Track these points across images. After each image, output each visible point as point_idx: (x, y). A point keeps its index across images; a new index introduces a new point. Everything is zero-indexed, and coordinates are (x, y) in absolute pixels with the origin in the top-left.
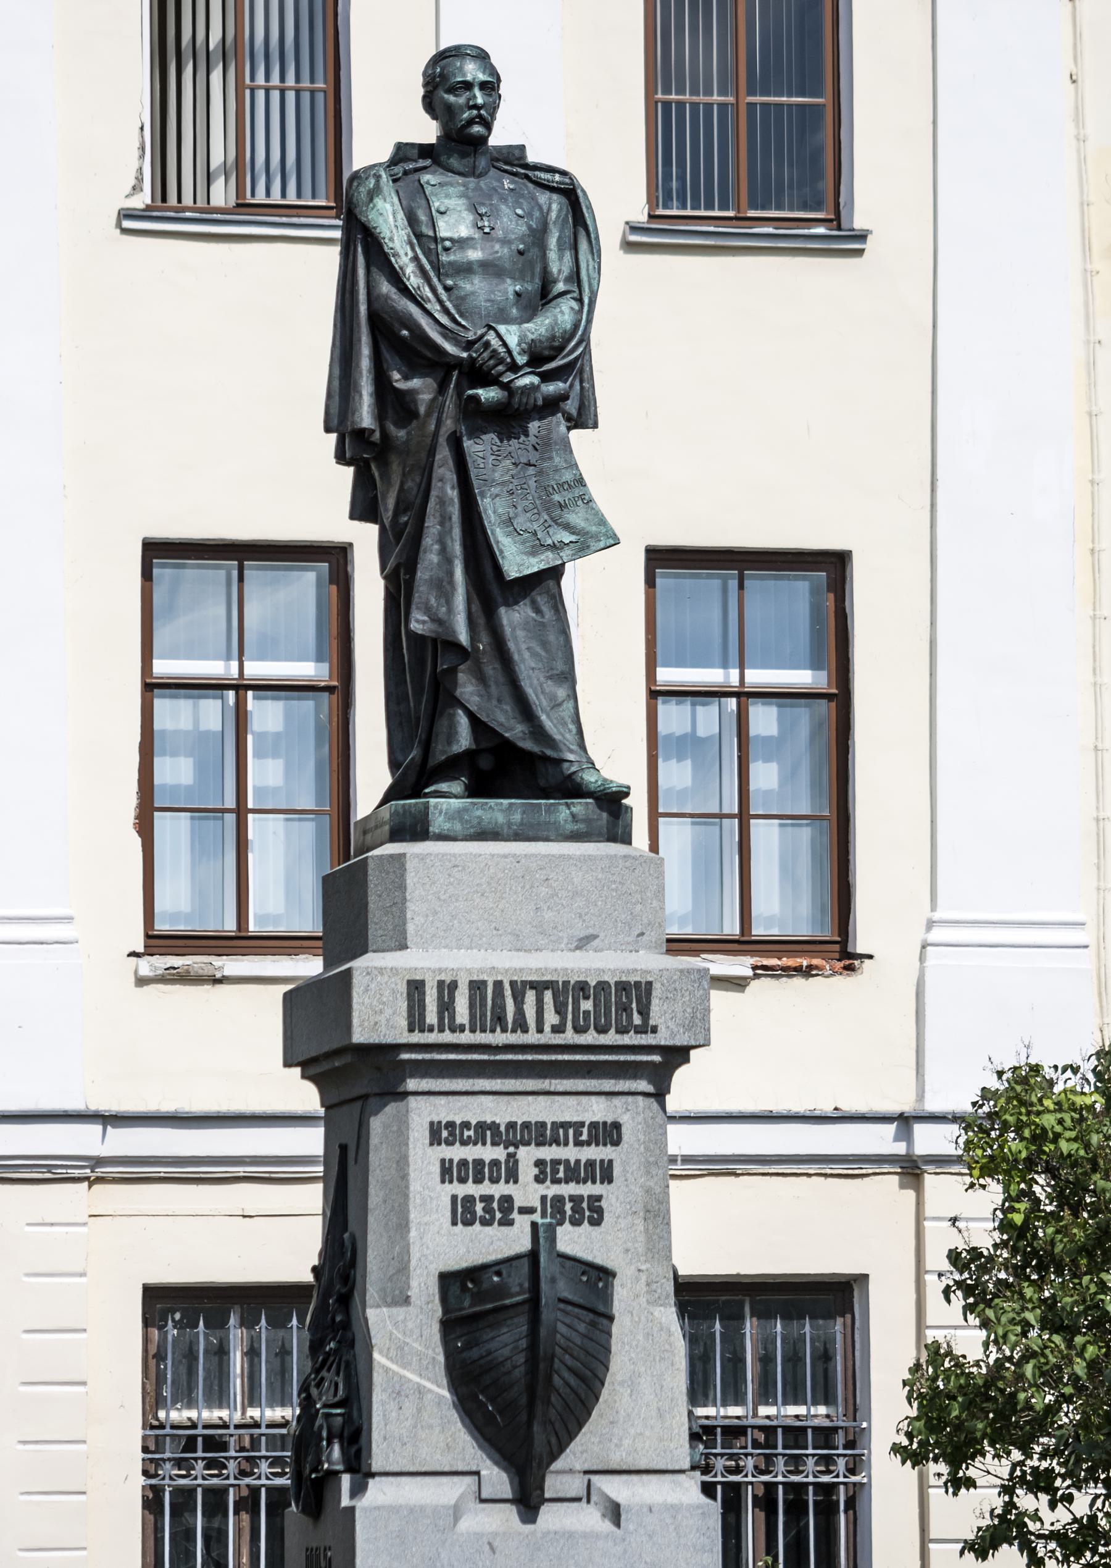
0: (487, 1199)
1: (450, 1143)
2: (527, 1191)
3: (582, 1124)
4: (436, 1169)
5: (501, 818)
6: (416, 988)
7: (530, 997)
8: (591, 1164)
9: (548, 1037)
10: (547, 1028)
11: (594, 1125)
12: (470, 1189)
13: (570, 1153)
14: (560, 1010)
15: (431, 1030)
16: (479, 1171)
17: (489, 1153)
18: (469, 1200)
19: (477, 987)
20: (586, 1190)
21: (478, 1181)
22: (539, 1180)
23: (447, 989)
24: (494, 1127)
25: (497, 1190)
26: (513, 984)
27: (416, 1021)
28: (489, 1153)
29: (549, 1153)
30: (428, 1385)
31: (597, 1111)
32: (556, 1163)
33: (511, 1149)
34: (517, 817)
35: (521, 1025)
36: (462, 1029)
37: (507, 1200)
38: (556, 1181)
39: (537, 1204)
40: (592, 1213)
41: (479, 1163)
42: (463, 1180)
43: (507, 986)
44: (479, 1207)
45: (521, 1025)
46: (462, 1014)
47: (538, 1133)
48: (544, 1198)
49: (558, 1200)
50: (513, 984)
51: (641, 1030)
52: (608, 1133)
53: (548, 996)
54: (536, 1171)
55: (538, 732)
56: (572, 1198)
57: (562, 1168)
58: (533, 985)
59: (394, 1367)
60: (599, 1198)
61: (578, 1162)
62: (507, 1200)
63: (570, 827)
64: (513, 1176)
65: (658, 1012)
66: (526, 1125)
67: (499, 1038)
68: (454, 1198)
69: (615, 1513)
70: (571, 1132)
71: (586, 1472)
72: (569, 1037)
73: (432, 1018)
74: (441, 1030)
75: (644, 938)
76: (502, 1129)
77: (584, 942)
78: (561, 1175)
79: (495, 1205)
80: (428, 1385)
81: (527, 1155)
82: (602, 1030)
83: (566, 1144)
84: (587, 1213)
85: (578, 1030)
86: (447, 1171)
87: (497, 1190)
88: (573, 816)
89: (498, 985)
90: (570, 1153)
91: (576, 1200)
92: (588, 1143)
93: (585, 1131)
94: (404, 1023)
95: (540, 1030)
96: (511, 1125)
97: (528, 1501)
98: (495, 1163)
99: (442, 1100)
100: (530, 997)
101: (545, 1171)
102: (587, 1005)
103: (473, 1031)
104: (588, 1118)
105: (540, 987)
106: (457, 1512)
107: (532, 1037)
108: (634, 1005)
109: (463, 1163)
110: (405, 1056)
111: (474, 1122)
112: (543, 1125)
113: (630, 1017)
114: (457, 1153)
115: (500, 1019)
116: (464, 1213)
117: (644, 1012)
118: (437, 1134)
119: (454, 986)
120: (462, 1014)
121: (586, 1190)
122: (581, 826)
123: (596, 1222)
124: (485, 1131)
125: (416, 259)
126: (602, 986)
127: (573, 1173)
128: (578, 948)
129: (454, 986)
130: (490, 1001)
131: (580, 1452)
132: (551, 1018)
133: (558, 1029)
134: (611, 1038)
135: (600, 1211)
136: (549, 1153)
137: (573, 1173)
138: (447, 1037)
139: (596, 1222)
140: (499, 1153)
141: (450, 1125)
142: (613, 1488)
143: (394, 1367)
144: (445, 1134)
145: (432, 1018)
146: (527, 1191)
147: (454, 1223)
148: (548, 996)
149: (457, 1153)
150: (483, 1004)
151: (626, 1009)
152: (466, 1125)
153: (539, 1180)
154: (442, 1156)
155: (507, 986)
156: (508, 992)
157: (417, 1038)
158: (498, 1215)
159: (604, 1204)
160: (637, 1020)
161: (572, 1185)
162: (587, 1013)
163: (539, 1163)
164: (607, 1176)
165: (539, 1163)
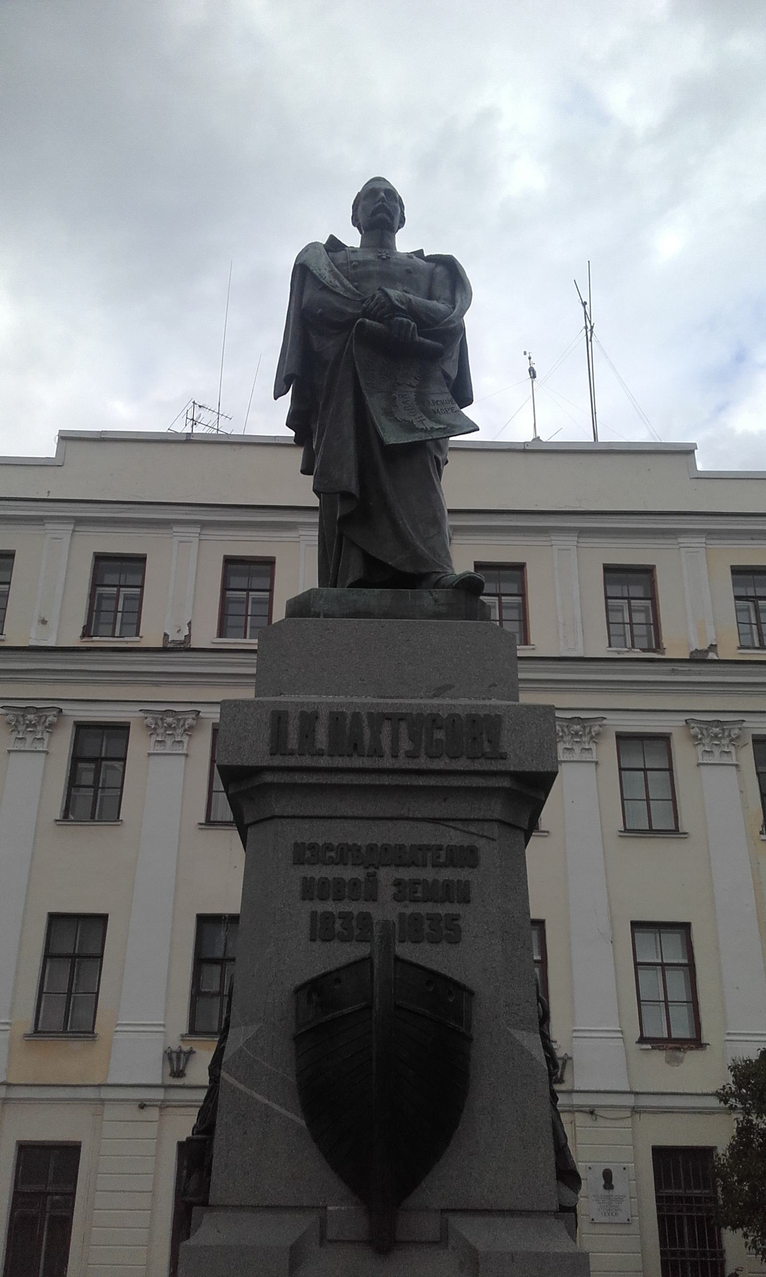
0: (345, 916)
3: (440, 848)
4: (297, 888)
6: (279, 719)
8: (448, 885)
9: (403, 763)
10: (401, 754)
11: (451, 849)
12: (330, 906)
13: (428, 874)
14: (413, 737)
15: (292, 754)
17: (349, 873)
18: (328, 917)
19: (336, 718)
20: (443, 909)
21: (338, 899)
22: (397, 898)
23: (309, 719)
25: (354, 908)
27: (278, 746)
28: (349, 873)
29: (406, 874)
30: (276, 1107)
31: (453, 837)
32: (416, 882)
33: (371, 870)
35: (377, 752)
36: (320, 754)
37: (365, 918)
38: (416, 901)
41: (339, 882)
43: (365, 718)
44: (338, 926)
45: (377, 752)
47: (399, 856)
48: (402, 915)
49: (416, 918)
50: (370, 715)
52: (466, 857)
54: (394, 890)
56: (431, 917)
57: (420, 888)
58: (388, 717)
59: (242, 1087)
60: (455, 918)
65: (507, 743)
66: (386, 848)
67: (358, 762)
68: (314, 914)
69: (472, 1260)
70: (430, 854)
71: (443, 1211)
72: (423, 763)
73: (293, 742)
74: (301, 755)
76: (364, 850)
77: (440, 692)
79: (354, 923)
80: (276, 1107)
81: (386, 876)
83: (425, 866)
86: (311, 890)
87: (354, 908)
88: (436, 601)
89: (356, 716)
90: (428, 874)
91: (433, 918)
92: (445, 866)
93: (443, 853)
94: (266, 748)
95: (395, 756)
96: (371, 848)
98: (355, 883)
99: (306, 824)
100: (387, 729)
101: (404, 891)
102: (440, 735)
103: (331, 755)
104: (445, 842)
106: (296, 1255)
107: (387, 763)
109: (324, 882)
110: (269, 778)
111: (336, 844)
112: (401, 847)
114: (318, 872)
116: (323, 930)
119: (315, 716)
121: (443, 909)
124: (345, 854)
125: (331, 271)
129: (315, 716)
130: (346, 731)
131: (440, 1186)
132: (406, 745)
133: (412, 755)
134: (462, 764)
135: (458, 930)
136: (406, 874)
138: (307, 761)
139: (455, 940)
140: (359, 873)
141: (313, 847)
142: (470, 1230)
143: (242, 1087)
145: (293, 742)
146: (386, 910)
147: (313, 940)
149: (318, 872)
152: (328, 847)
153: (397, 898)
154: (303, 875)
156: (365, 723)
157: (278, 761)
159: (461, 923)
160: (487, 748)
161: (430, 904)
163: (398, 883)
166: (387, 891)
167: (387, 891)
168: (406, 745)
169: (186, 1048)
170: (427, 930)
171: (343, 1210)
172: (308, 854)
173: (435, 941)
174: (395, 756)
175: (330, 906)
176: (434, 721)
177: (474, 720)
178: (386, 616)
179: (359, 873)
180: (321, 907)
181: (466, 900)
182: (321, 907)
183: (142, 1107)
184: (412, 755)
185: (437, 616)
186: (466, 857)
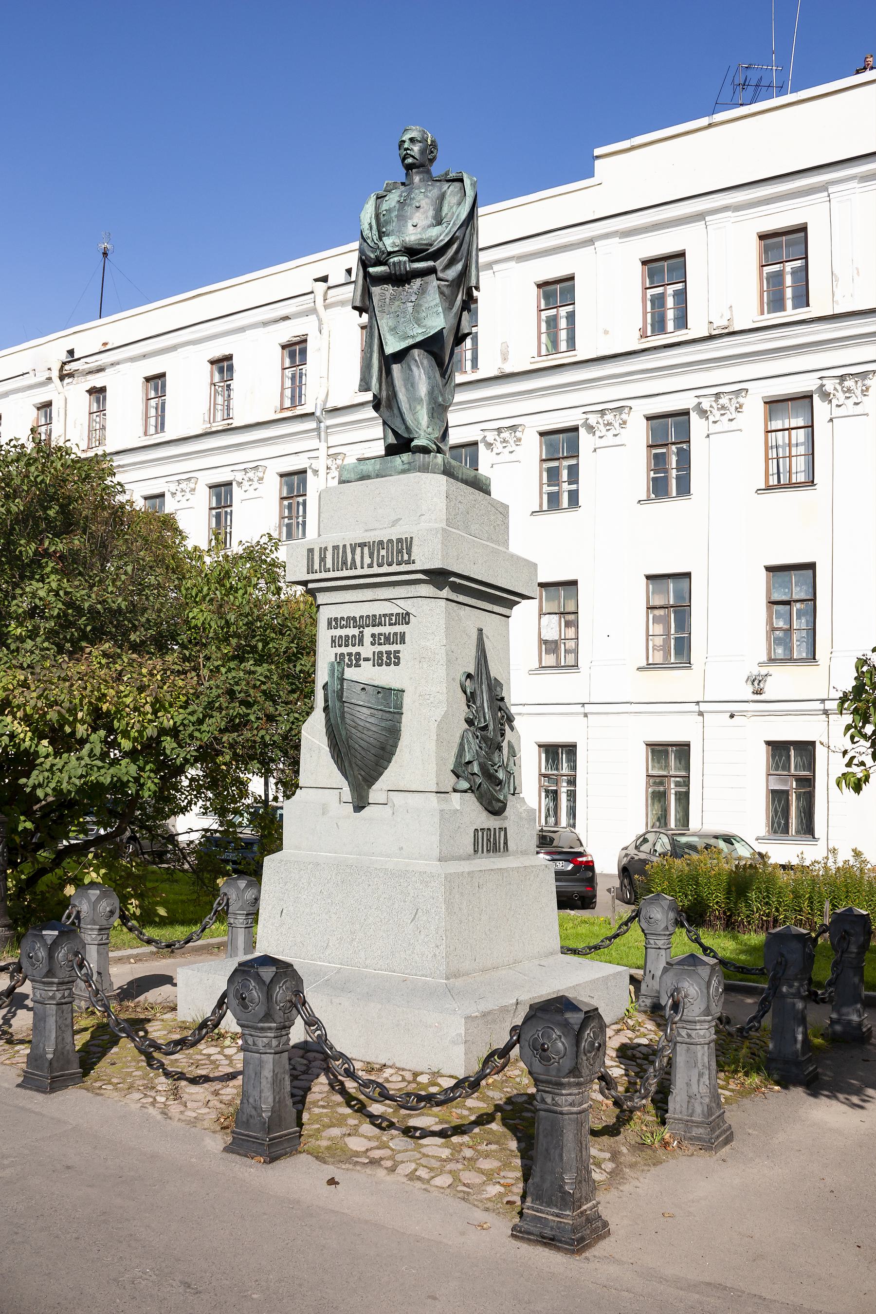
0: (350, 654)
1: (336, 628)
2: (367, 650)
3: (392, 615)
5: (371, 469)
7: (358, 550)
8: (395, 634)
9: (367, 571)
10: (365, 566)
12: (344, 650)
13: (386, 630)
14: (371, 556)
16: (346, 641)
17: (353, 631)
22: (373, 644)
24: (354, 618)
26: (351, 545)
28: (353, 631)
29: (377, 630)
34: (378, 467)
35: (354, 566)
37: (358, 654)
38: (380, 644)
39: (371, 656)
40: (393, 659)
42: (340, 646)
45: (354, 566)
46: (329, 564)
47: (375, 621)
49: (380, 653)
51: (408, 563)
52: (405, 618)
53: (366, 549)
55: (407, 428)
57: (382, 637)
60: (398, 652)
61: (390, 633)
62: (358, 654)
63: (401, 467)
64: (361, 642)
66: (368, 616)
68: (336, 654)
70: (387, 618)
72: (376, 570)
75: (423, 517)
78: (382, 641)
79: (353, 658)
81: (368, 631)
82: (390, 565)
84: (393, 659)
85: (380, 565)
91: (388, 653)
93: (394, 618)
95: (362, 568)
97: (360, 804)
98: (354, 636)
102: (383, 552)
103: (334, 571)
105: (362, 545)
107: (359, 572)
108: (405, 551)
109: (341, 637)
112: (375, 616)
113: (402, 556)
115: (345, 563)
117: (409, 553)
118: (332, 623)
120: (329, 564)
122: (406, 466)
123: (397, 664)
124: (351, 621)
126: (390, 541)
127: (388, 640)
128: (393, 526)
130: (342, 556)
132: (367, 560)
133: (370, 566)
134: (394, 568)
135: (398, 658)
136: (377, 630)
137: (388, 640)
140: (355, 631)
141: (336, 619)
144: (334, 623)
146: (367, 650)
148: (366, 549)
150: (338, 558)
151: (400, 552)
152: (342, 618)
153: (373, 644)
155: (348, 547)
158: (354, 662)
160: (406, 557)
161: (387, 646)
162: (383, 556)
163: (373, 635)
164: (402, 639)
165: (373, 635)
166: (368, 639)
167: (368, 639)
168: (367, 560)
169: (764, 671)
170: (384, 658)
171: (347, 793)
172: (334, 623)
173: (388, 665)
174: (362, 568)
175: (344, 650)
176: (381, 543)
177: (399, 540)
178: (378, 476)
179: (355, 631)
180: (339, 650)
181: (403, 641)
182: (339, 650)
183: (732, 716)
184: (370, 566)
185: (404, 472)
186: (405, 618)
